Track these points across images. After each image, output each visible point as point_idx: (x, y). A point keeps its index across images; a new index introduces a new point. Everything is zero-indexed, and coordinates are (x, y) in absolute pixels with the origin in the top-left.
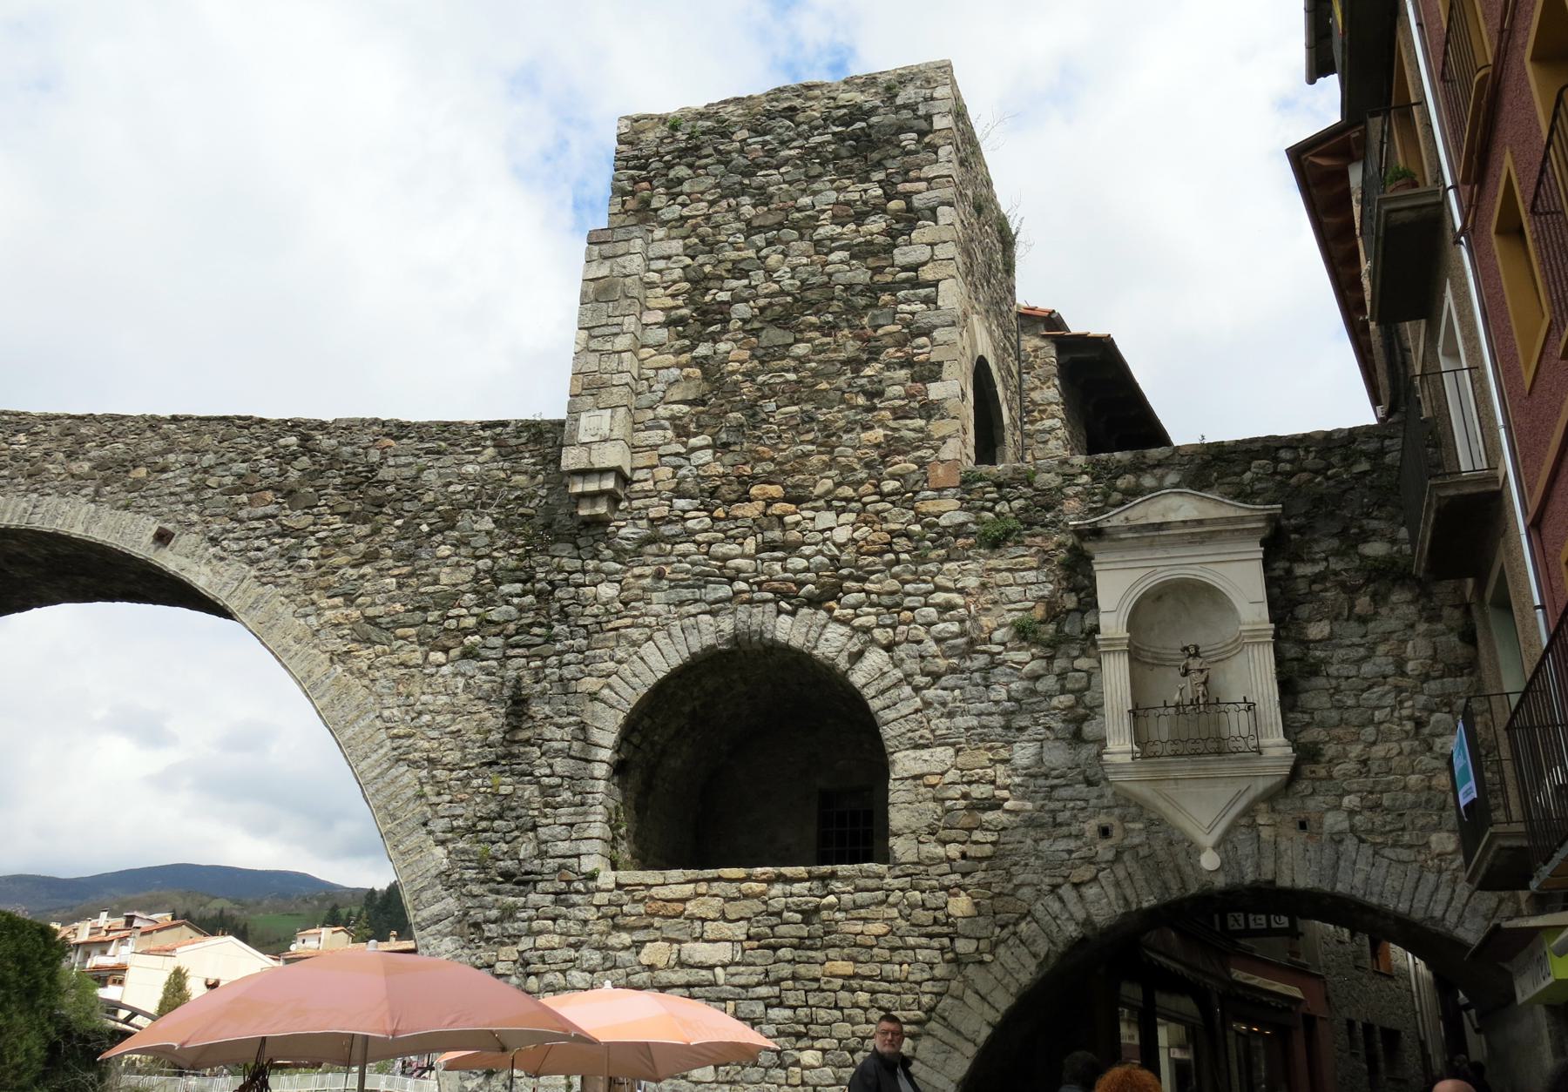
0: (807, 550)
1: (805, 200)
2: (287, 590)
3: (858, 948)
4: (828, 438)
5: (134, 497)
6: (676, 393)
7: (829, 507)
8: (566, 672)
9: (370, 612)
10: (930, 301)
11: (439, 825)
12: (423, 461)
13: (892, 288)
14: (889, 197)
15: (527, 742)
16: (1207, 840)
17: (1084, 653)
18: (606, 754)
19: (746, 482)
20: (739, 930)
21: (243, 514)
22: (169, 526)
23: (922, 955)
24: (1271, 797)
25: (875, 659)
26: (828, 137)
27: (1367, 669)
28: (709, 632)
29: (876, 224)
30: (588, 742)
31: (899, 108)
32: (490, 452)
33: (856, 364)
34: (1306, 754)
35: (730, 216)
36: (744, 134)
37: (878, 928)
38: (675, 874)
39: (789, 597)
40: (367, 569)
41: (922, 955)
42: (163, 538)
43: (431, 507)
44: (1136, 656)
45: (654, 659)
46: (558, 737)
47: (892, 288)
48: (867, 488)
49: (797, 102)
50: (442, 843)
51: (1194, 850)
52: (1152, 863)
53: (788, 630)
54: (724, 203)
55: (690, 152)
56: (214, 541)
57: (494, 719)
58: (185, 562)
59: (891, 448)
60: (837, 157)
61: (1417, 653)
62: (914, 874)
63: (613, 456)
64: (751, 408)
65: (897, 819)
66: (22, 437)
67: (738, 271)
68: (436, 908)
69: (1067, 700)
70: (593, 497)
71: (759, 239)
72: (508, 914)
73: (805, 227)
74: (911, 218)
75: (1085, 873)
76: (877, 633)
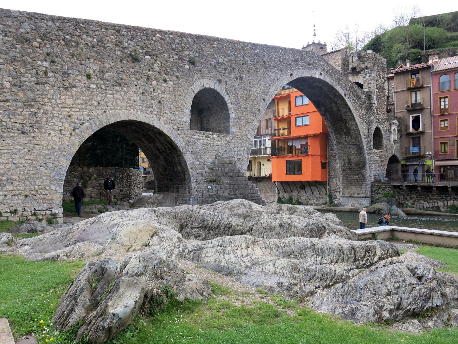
19: (378, 108)
20: (379, 156)
42: (345, 95)
53: (380, 126)
57: (367, 131)
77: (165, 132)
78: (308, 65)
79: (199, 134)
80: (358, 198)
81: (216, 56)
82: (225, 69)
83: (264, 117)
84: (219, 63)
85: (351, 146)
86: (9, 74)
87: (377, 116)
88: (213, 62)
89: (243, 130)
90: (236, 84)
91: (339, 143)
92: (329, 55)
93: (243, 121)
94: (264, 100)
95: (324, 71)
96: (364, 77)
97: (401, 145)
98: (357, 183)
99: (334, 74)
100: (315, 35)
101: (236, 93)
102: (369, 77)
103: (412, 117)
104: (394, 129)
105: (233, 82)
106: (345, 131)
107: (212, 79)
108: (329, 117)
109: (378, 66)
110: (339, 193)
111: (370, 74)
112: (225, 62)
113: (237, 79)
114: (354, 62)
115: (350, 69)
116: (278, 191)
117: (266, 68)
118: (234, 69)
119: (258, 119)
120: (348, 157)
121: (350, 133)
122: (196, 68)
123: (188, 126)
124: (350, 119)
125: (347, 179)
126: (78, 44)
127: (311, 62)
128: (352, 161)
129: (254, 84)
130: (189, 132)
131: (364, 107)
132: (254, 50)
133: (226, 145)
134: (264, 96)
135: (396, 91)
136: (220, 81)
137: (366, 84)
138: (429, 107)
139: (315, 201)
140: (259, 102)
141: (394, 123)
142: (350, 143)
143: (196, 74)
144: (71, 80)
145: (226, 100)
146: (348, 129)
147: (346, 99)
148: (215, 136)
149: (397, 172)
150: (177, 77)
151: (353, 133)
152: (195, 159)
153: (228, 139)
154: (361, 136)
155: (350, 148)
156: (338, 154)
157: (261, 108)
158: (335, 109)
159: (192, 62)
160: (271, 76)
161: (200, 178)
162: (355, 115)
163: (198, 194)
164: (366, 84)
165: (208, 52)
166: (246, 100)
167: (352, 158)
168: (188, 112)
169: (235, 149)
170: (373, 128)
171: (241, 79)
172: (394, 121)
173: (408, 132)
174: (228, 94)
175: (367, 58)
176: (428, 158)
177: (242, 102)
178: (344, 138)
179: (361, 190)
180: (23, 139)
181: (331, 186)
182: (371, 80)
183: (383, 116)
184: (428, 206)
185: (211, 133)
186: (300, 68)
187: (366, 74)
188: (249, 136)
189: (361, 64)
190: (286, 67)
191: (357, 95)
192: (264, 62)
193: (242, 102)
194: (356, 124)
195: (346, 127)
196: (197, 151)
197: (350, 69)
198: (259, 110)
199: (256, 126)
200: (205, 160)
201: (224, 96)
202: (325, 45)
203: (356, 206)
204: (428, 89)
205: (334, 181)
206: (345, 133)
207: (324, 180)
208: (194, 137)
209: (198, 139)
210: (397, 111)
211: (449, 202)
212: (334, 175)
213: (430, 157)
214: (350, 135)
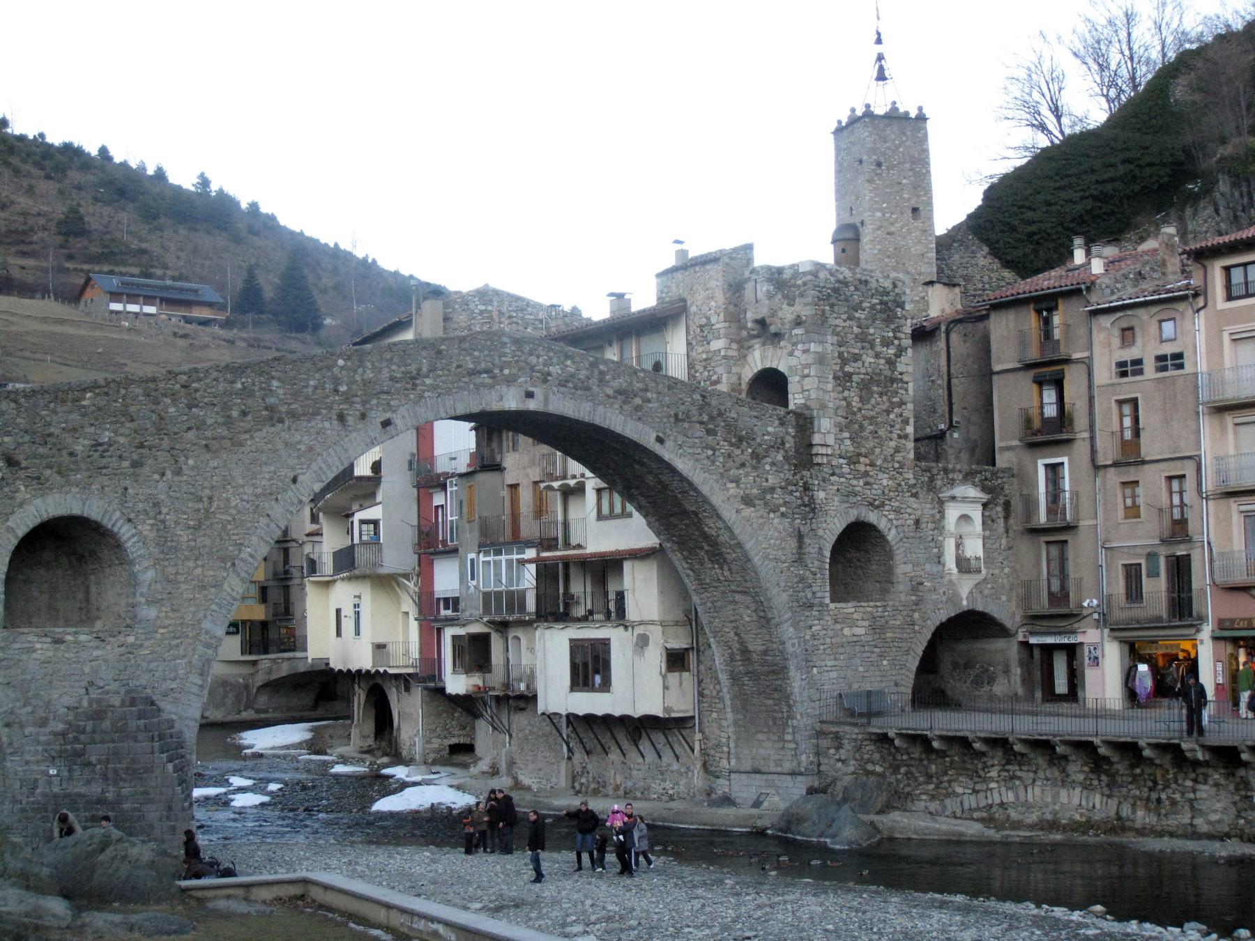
0: (877, 487)
1: (872, 331)
2: (714, 477)
4: (881, 445)
5: (639, 413)
6: (840, 412)
7: (880, 470)
8: (814, 526)
9: (747, 492)
10: (906, 390)
11: (782, 584)
12: (754, 420)
14: (896, 338)
15: (804, 554)
16: (964, 596)
17: (941, 535)
18: (828, 560)
19: (859, 455)
20: (866, 623)
21: (690, 435)
22: (660, 434)
23: (908, 631)
24: (976, 585)
25: (893, 532)
26: (877, 301)
27: (994, 546)
28: (852, 516)
30: (822, 555)
31: (897, 294)
32: (777, 422)
33: (888, 412)
35: (850, 331)
36: (852, 288)
37: (898, 623)
38: (850, 605)
40: (741, 471)
41: (908, 631)
42: (660, 440)
43: (760, 445)
45: (838, 525)
48: (890, 465)
49: (868, 278)
50: (784, 591)
51: (962, 599)
53: (872, 517)
54: (847, 323)
56: (681, 446)
57: (792, 543)
58: (672, 456)
59: (897, 450)
60: (881, 311)
63: (830, 440)
66: (569, 362)
67: (856, 358)
68: (787, 616)
69: (935, 550)
70: (822, 455)
71: (859, 345)
73: (872, 347)
74: (900, 351)
75: (940, 606)
76: (894, 522)
78: (466, 379)
79: (31, 638)
80: (775, 777)
81: (92, 430)
83: (527, 475)
84: (100, 445)
85: (738, 597)
87: (855, 482)
88: (80, 448)
89: (183, 610)
91: (703, 586)
92: (691, 270)
93: (183, 586)
95: (545, 381)
96: (791, 354)
97: (1014, 570)
98: (771, 723)
99: (601, 381)
100: (881, 77)
101: (160, 513)
102: (804, 357)
103: (1046, 466)
104: (965, 518)
105: (149, 487)
106: (706, 548)
107: (77, 490)
108: (643, 502)
109: (856, 308)
110: (728, 759)
111: (807, 346)
112: (122, 440)
114: (759, 299)
115: (750, 325)
116: (570, 750)
119: (243, 574)
120: (736, 634)
121: (721, 554)
122: (22, 474)
124: (705, 511)
125: (745, 709)
127: (483, 365)
128: (751, 648)
131: (773, 464)
132: (233, 382)
133: (123, 658)
135: (996, 368)
137: (797, 378)
138: (1086, 435)
139: (668, 785)
140: (249, 525)
141: (953, 498)
142: (733, 588)
143: (23, 488)
145: (125, 538)
146: (714, 543)
147: (667, 453)
148: (83, 638)
149: (1007, 671)
151: (731, 556)
152: (18, 700)
153: (131, 639)
154: (754, 568)
155: (734, 602)
156: (710, 623)
158: (650, 480)
160: (299, 443)
161: (32, 748)
162: (717, 499)
163: (25, 789)
164: (797, 378)
165: (63, 425)
166: (197, 528)
167: (748, 638)
169: (156, 664)
170: (832, 526)
171: (178, 472)
172: (960, 490)
173: (1033, 524)
174: (129, 520)
175: (799, 286)
176: (1089, 618)
177: (184, 536)
178: (713, 572)
179: (783, 748)
181: (707, 730)
182: (808, 366)
184: (974, 805)
185: (69, 630)
186: (426, 394)
187: (794, 344)
188: (206, 625)
189: (785, 306)
190: (364, 403)
191: (730, 427)
192: (271, 409)
193: (184, 536)
194: (729, 529)
195: (706, 537)
196: (24, 680)
197: (750, 325)
199: (234, 594)
200: (49, 702)
201: (115, 529)
202: (921, 118)
203: (766, 804)
204: (1083, 368)
205: (715, 715)
206: (707, 552)
208: (18, 646)
209: (31, 650)
210: (1003, 444)
211: (1030, 790)
212: (714, 693)
213: (1096, 616)
214: (725, 560)
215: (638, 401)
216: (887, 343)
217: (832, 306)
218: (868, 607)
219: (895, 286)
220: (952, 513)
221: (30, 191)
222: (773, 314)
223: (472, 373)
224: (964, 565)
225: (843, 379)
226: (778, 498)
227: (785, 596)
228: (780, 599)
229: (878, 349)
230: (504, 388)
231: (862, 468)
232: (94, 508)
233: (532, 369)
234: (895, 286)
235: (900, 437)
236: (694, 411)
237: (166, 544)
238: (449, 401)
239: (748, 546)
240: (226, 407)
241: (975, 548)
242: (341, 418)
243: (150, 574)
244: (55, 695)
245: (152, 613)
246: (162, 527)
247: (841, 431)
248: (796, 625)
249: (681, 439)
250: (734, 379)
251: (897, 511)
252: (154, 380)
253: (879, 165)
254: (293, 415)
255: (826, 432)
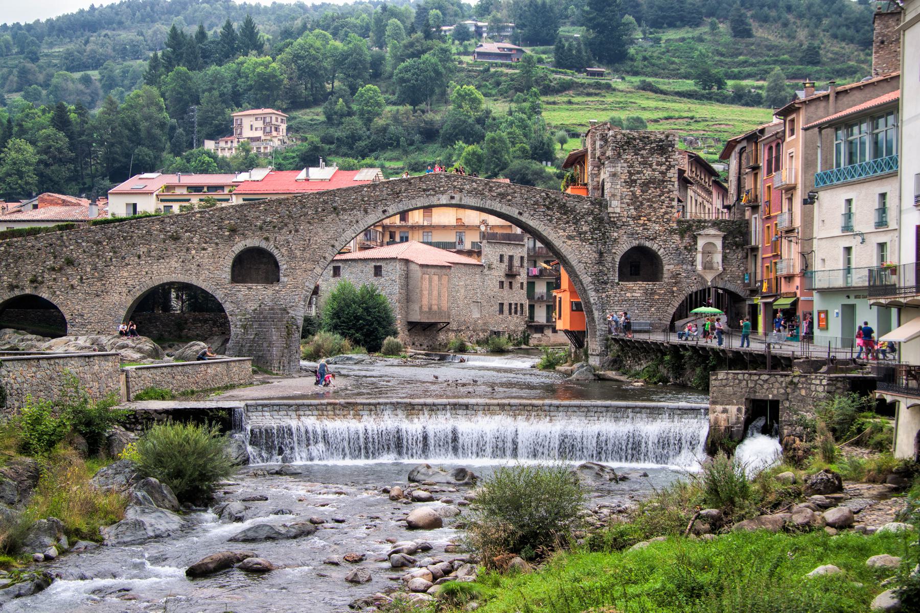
3: (659, 294)
4: (655, 210)
5: (510, 203)
13: (666, 181)
24: (719, 275)
28: (635, 243)
29: (664, 167)
33: (660, 196)
34: (724, 269)
39: (647, 238)
42: (520, 214)
44: (703, 253)
46: (609, 259)
47: (666, 181)
52: (702, 284)
53: (648, 244)
55: (628, 143)
57: (596, 256)
59: (666, 213)
61: (740, 256)
62: (668, 284)
63: (618, 210)
64: (642, 204)
65: (665, 276)
67: (639, 173)
72: (603, 288)
73: (651, 166)
74: (670, 167)
77: (203, 287)
82: (274, 227)
86: (89, 263)
90: (290, 238)
94: (333, 246)
99: (490, 191)
113: (290, 232)
117: (338, 214)
118: (286, 225)
123: (227, 281)
126: (132, 237)
129: (316, 233)
130: (229, 286)
131: (586, 222)
134: (332, 242)
136: (267, 239)
144: (127, 261)
150: (217, 244)
157: (327, 255)
159: (233, 231)
168: (228, 270)
171: (297, 231)
180: (97, 299)
183: (663, 226)
188: (307, 284)
192: (335, 209)
193: (298, 253)
198: (324, 258)
207: (576, 329)
215: (510, 197)
216: (660, 164)
217: (624, 150)
218: (644, 284)
219: (667, 137)
220: (701, 243)
221: (791, 37)
222: (603, 154)
223: (424, 190)
224: (708, 266)
225: (631, 183)
226: (588, 236)
227: (590, 279)
228: (587, 280)
229: (654, 167)
230: (440, 196)
231: (641, 222)
232: (264, 245)
233: (455, 187)
234: (667, 137)
235: (667, 207)
236: (541, 200)
237: (292, 256)
238: (413, 202)
239: (568, 257)
240: (317, 208)
241: (718, 258)
242: (366, 211)
243: (285, 266)
244: (248, 306)
245: (285, 279)
246: (290, 251)
247: (628, 205)
248: (597, 291)
249: (532, 213)
250: (595, 183)
251: (665, 241)
252: (288, 199)
253: (882, 42)
254: (344, 210)
255: (615, 207)
